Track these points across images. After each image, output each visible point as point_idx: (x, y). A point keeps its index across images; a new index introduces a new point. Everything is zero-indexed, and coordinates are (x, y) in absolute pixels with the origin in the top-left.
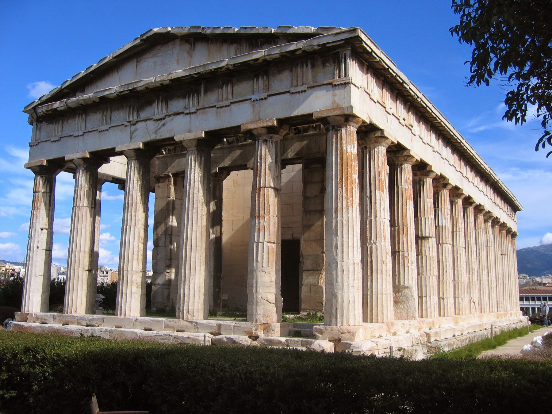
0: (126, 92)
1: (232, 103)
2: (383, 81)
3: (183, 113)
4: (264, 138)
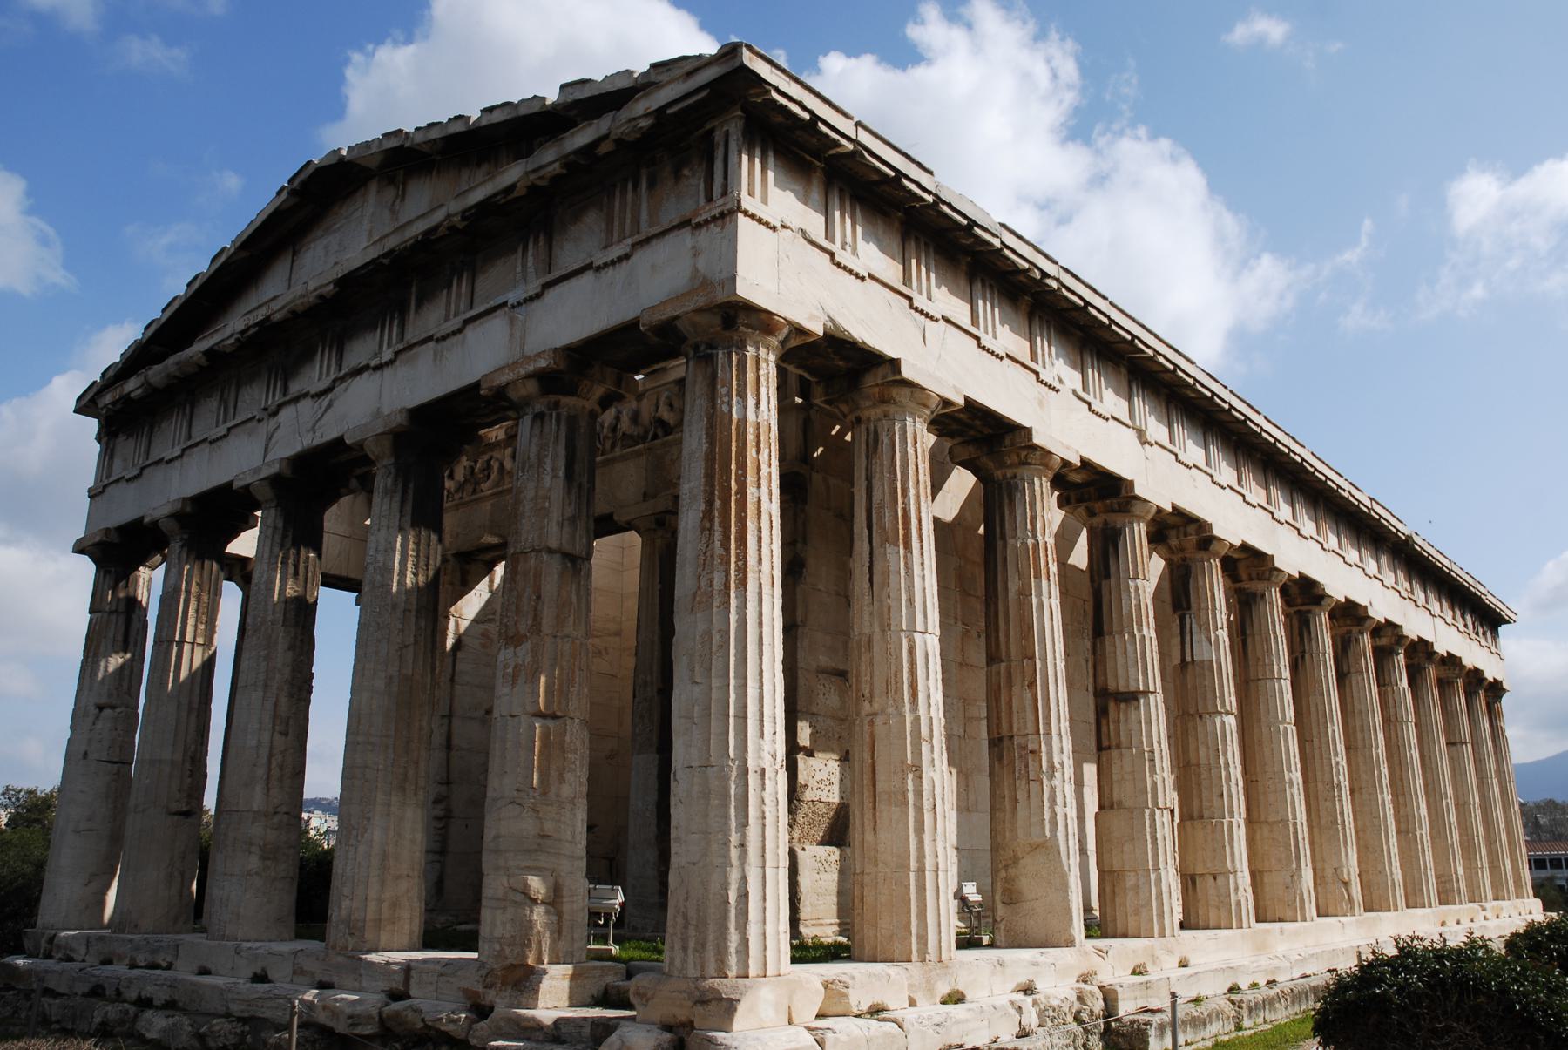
0: (252, 331)
1: (467, 322)
2: (902, 223)
3: (367, 367)
4: (538, 408)
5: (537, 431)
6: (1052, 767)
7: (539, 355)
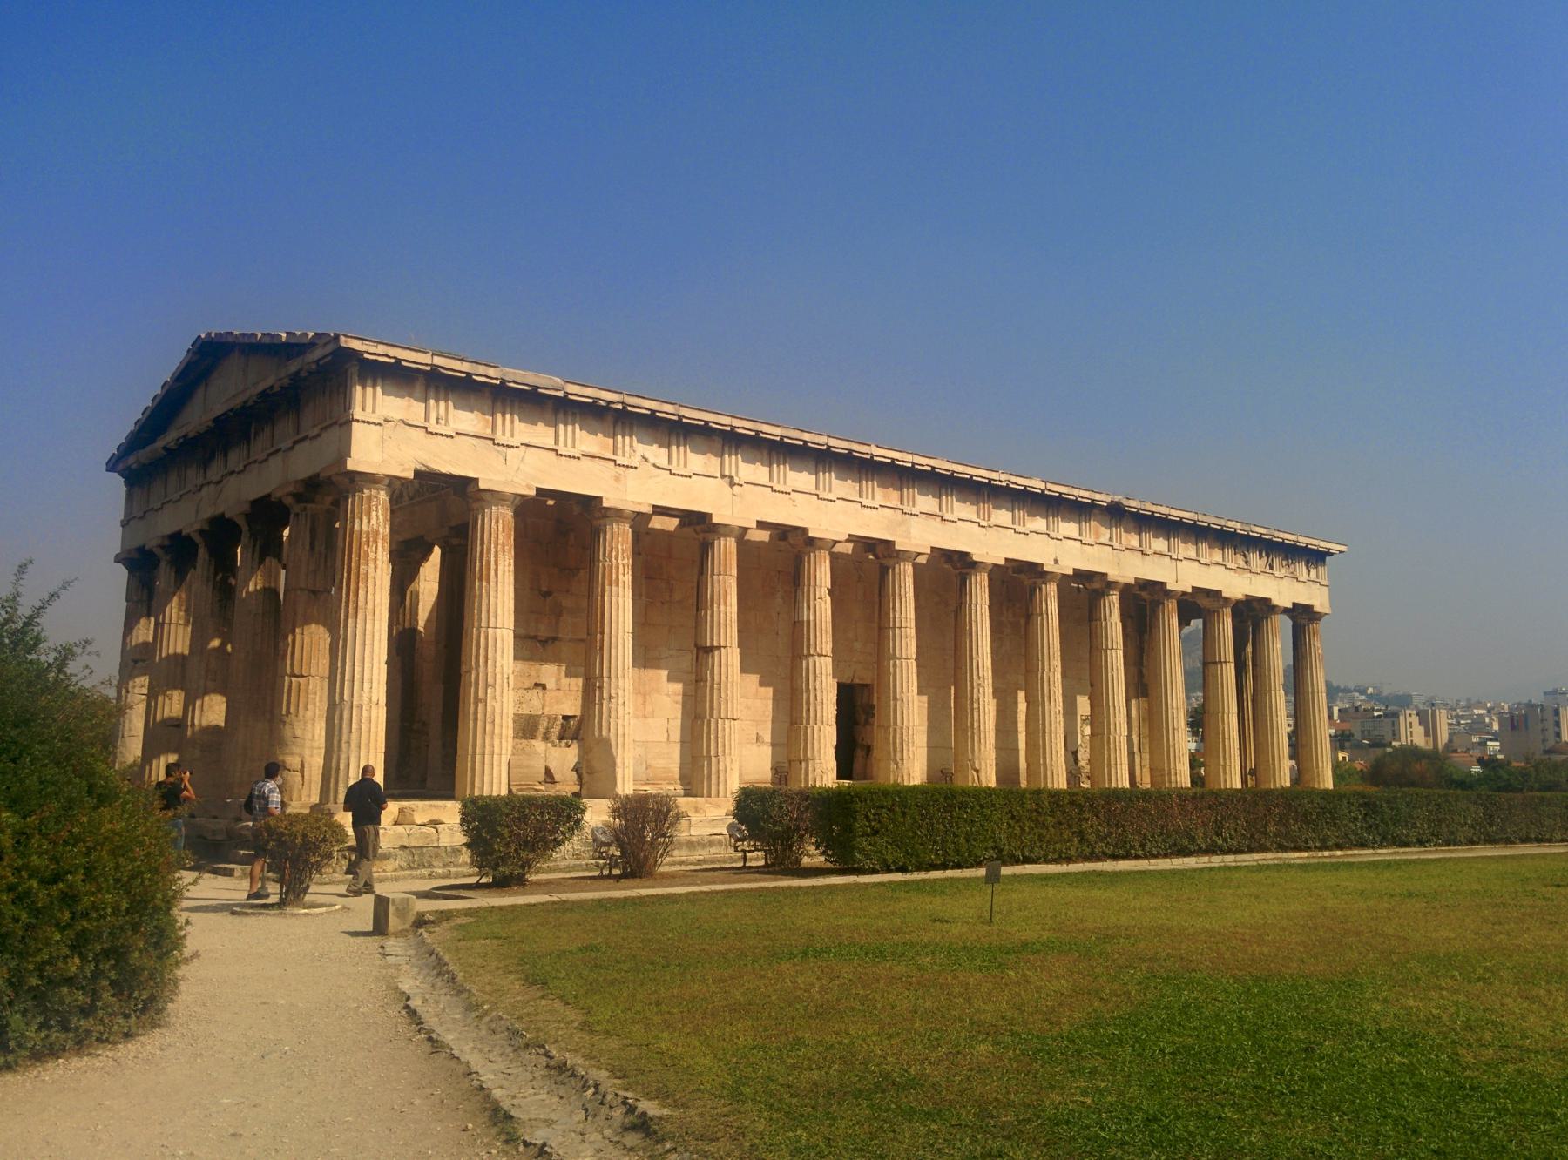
6: (610, 697)
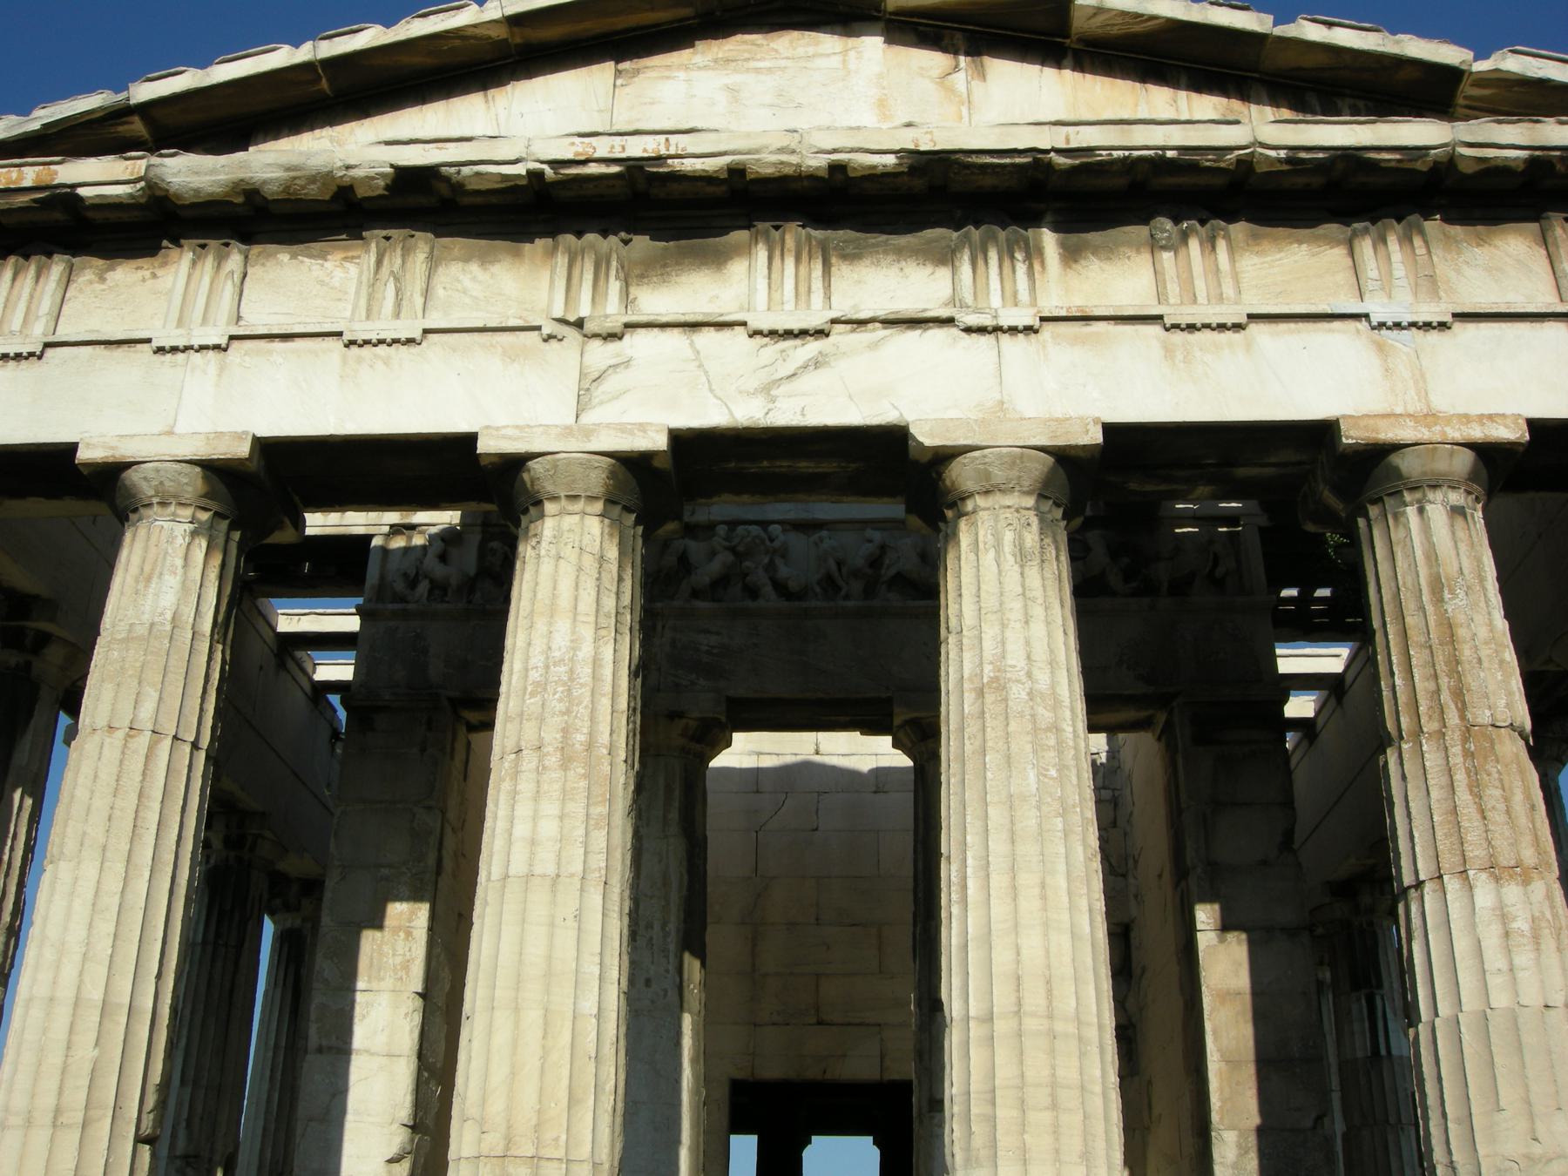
0: (593, 169)
1: (1252, 317)
3: (949, 321)
5: (1461, 534)
7: (1491, 417)
